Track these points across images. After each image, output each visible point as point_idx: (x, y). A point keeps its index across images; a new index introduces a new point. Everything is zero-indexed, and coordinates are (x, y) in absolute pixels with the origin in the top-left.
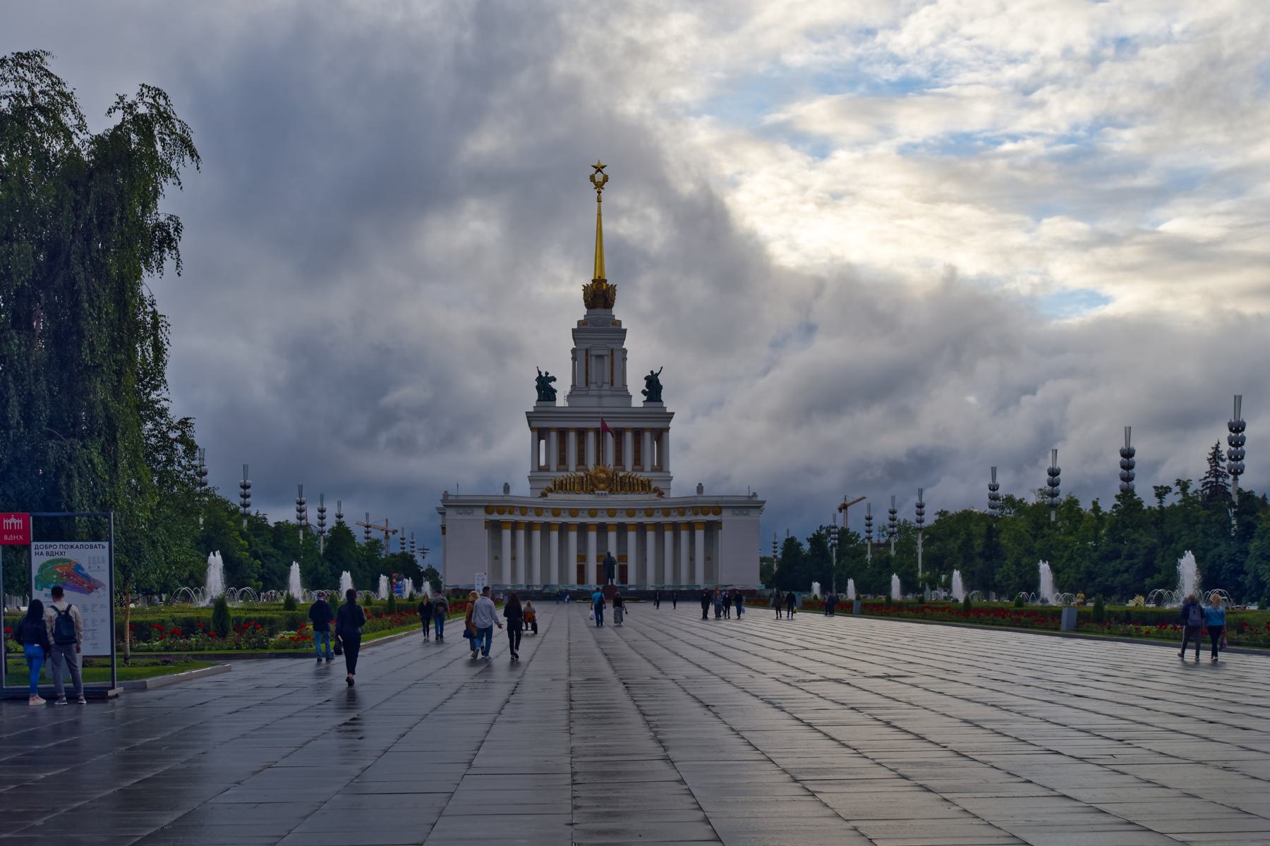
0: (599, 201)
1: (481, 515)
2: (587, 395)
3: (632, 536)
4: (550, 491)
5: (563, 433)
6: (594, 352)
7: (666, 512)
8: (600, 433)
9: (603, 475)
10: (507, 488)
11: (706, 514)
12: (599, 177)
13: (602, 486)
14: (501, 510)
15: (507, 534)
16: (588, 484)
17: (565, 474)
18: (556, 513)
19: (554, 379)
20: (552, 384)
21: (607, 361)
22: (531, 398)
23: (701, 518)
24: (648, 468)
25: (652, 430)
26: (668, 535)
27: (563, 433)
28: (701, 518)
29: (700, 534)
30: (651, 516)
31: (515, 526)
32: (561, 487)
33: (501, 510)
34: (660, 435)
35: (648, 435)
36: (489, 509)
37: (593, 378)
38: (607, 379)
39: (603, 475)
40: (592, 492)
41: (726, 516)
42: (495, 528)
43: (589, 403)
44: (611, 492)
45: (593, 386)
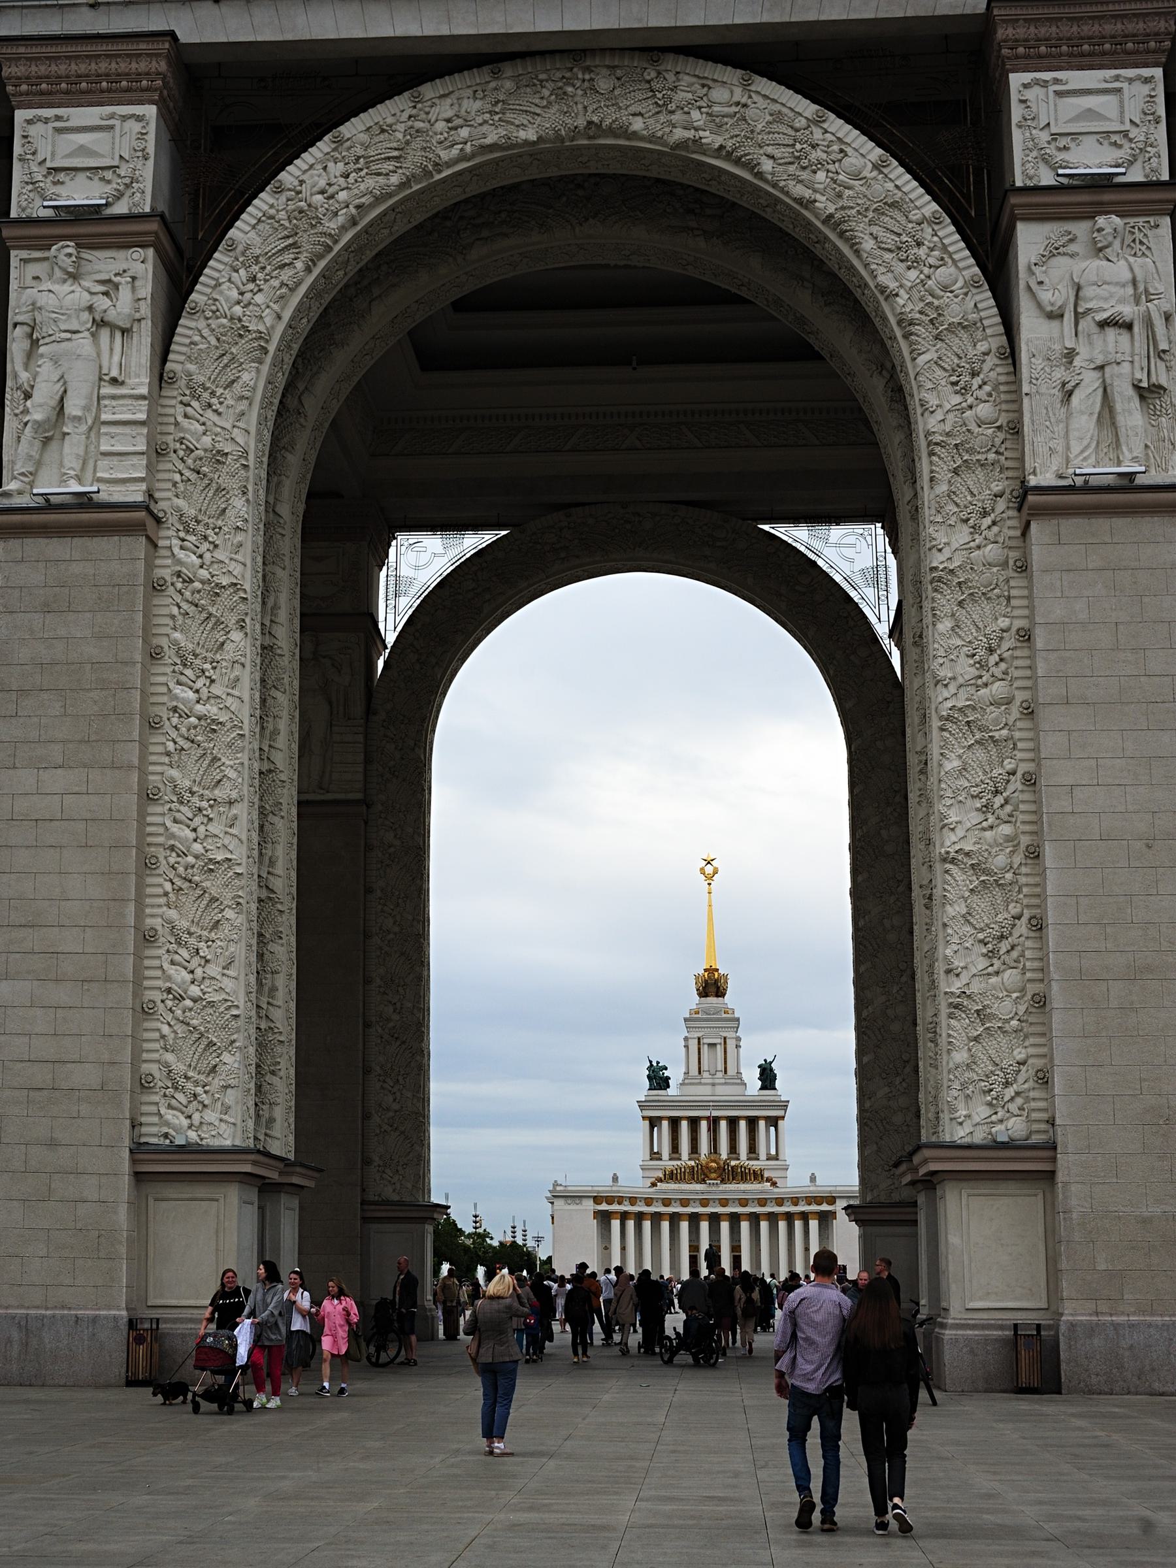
1: (589, 1205)
2: (700, 1084)
4: (660, 1180)
5: (675, 1122)
6: (706, 1041)
7: (780, 1202)
8: (714, 1122)
9: (714, 1165)
12: (709, 869)
14: (610, 1200)
15: (616, 1224)
16: (699, 1174)
17: (679, 1163)
18: (667, 1202)
21: (720, 1049)
23: (814, 1208)
24: (763, 1156)
25: (767, 1118)
27: (675, 1122)
28: (814, 1208)
29: (814, 1224)
31: (624, 1216)
32: (671, 1176)
33: (610, 1200)
34: (774, 1122)
35: (762, 1123)
36: (597, 1200)
37: (705, 1066)
38: (720, 1066)
39: (714, 1165)
40: (703, 1181)
42: (604, 1218)
43: (701, 1092)
44: (723, 1181)
45: (706, 1075)
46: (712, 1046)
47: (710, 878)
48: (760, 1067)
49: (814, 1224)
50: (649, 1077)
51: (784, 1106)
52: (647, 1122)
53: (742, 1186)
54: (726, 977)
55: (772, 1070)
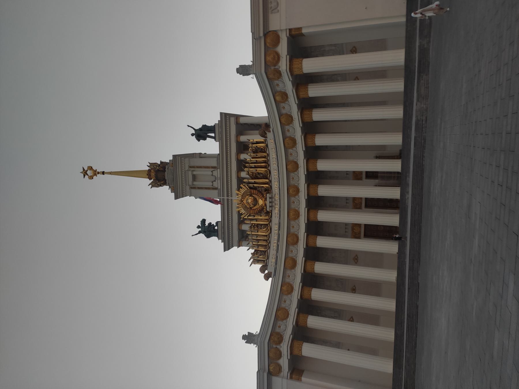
0: (103, 173)
3: (323, 165)
6: (190, 183)
7: (286, 120)
10: (249, 338)
11: (277, 57)
12: (89, 172)
13: (261, 202)
15: (308, 350)
19: (204, 221)
20: (207, 224)
22: (216, 243)
23: (283, 65)
26: (318, 115)
28: (283, 65)
29: (309, 65)
30: (294, 142)
35: (243, 138)
40: (269, 214)
41: (280, 23)
44: (269, 190)
45: (215, 184)
46: (194, 178)
47: (96, 173)
48: (199, 141)
49: (309, 65)
50: (208, 236)
51: (225, 117)
52: (244, 243)
53: (273, 166)
54: (152, 165)
55: (200, 129)
